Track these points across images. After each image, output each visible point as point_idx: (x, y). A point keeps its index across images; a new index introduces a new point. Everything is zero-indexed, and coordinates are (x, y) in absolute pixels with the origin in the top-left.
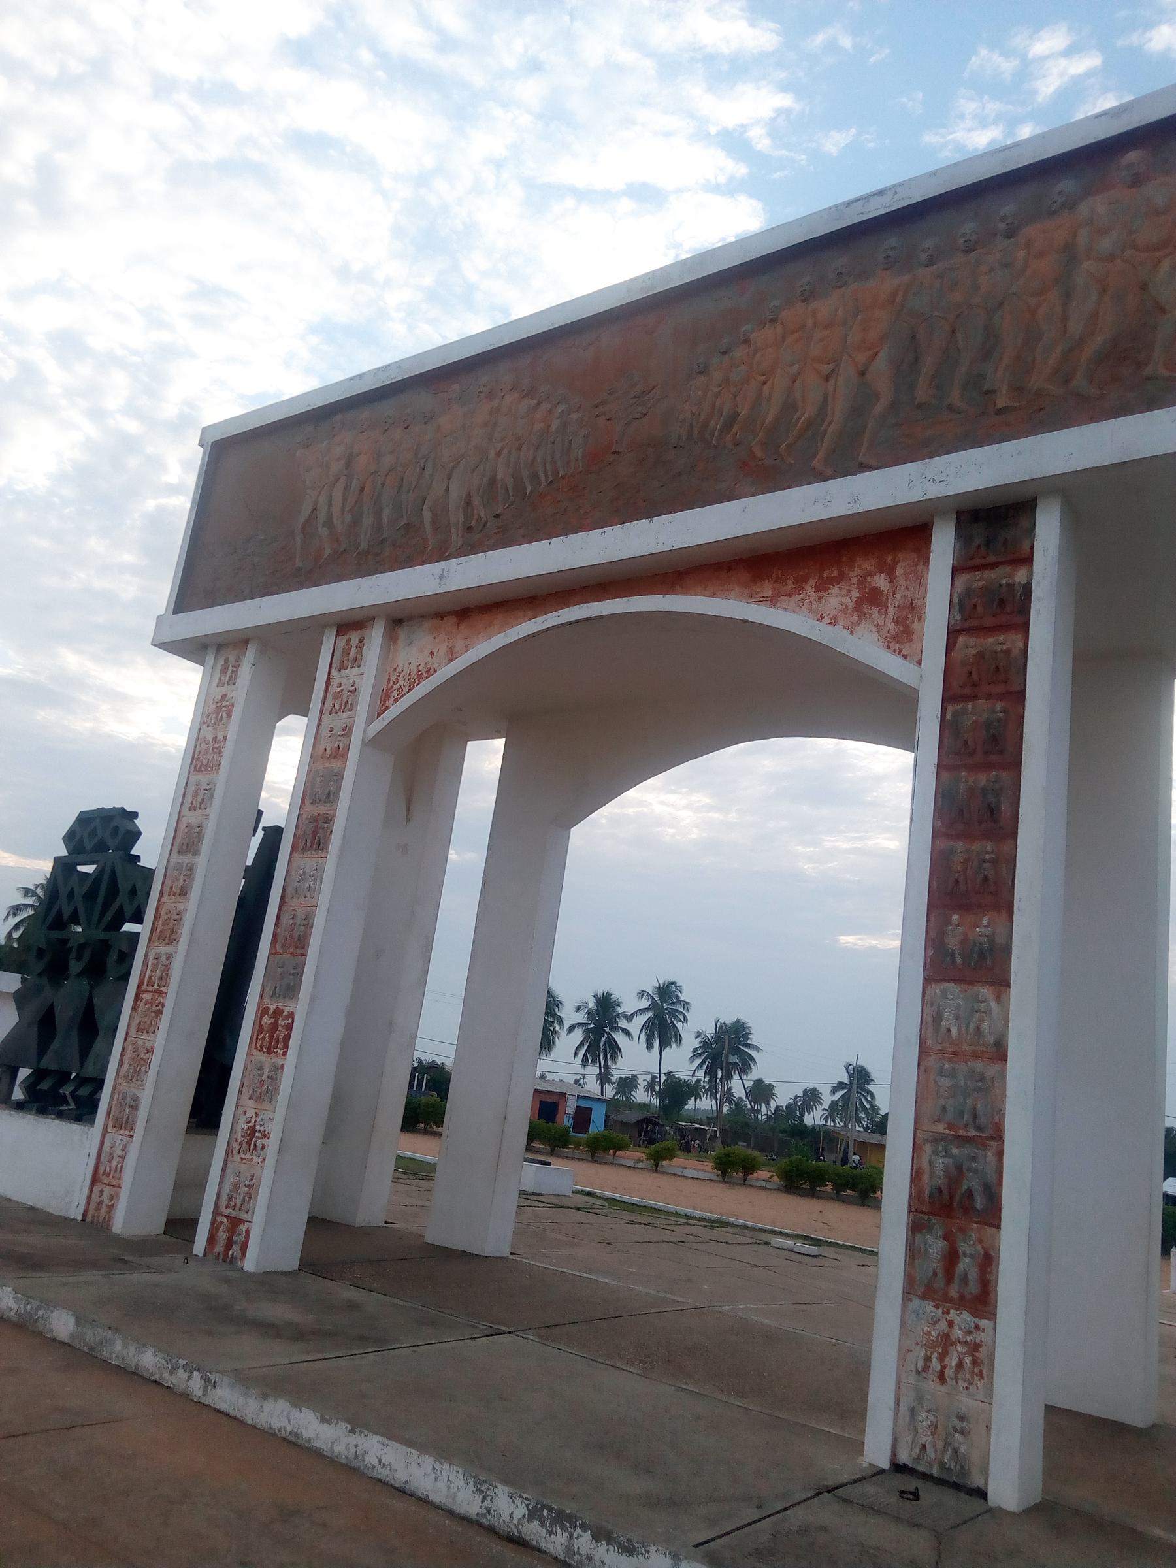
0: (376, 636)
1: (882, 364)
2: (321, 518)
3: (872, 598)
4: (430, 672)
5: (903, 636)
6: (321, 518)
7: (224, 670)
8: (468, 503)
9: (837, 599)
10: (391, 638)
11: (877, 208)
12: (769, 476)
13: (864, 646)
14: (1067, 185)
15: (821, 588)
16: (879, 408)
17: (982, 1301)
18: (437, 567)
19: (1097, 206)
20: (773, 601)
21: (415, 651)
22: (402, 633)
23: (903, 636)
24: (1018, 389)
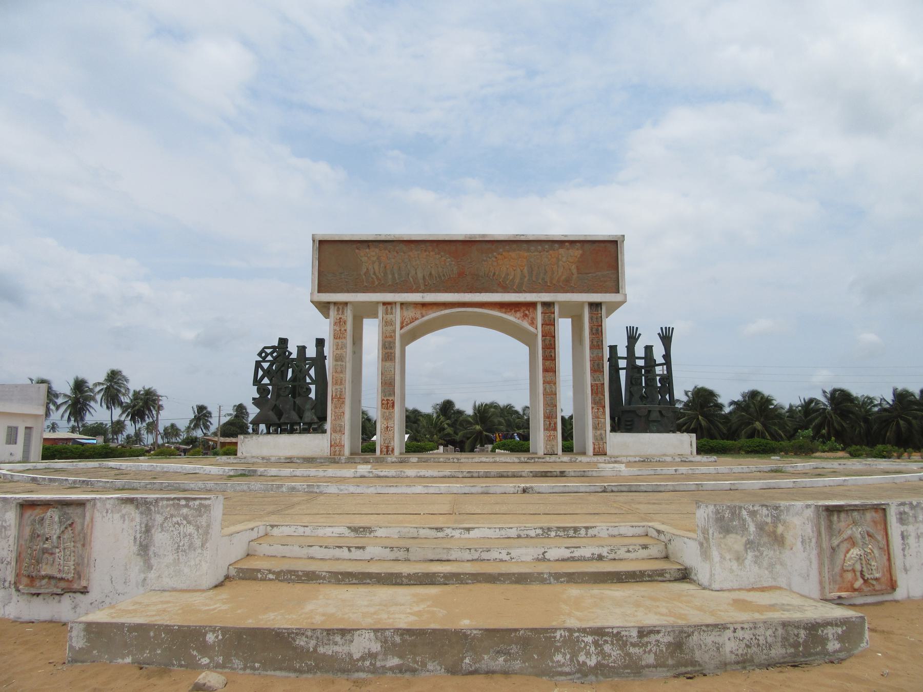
0: (398, 307)
1: (526, 271)
2: (372, 273)
3: (525, 315)
4: (416, 319)
5: (533, 323)
6: (372, 273)
7: (338, 310)
8: (424, 278)
9: (519, 314)
10: (401, 308)
11: (523, 238)
12: (505, 289)
13: (525, 324)
14: (557, 245)
15: (516, 311)
16: (526, 279)
17: (555, 429)
18: (421, 294)
19: (562, 251)
20: (505, 313)
21: (410, 313)
22: (404, 308)
23: (533, 323)
24: (551, 283)
